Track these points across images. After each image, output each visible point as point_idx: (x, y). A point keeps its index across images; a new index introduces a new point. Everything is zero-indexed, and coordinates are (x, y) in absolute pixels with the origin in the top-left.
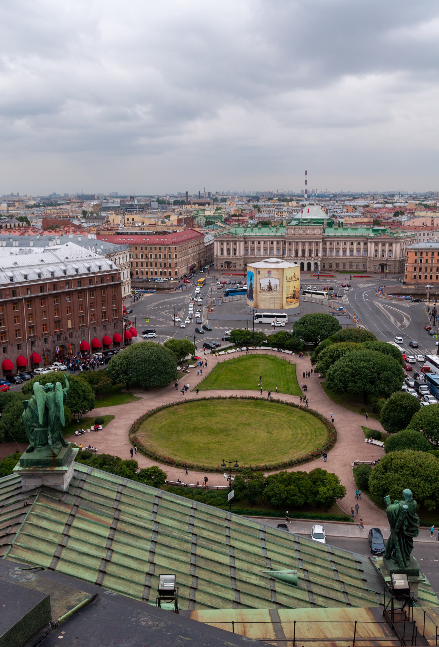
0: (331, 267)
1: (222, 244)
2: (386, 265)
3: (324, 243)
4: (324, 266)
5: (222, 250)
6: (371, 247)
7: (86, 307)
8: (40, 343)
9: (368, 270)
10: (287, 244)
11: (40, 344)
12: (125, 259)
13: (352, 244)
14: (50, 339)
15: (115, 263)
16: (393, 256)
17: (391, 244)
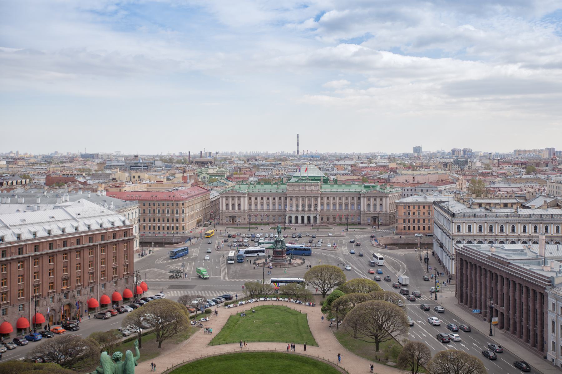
0: (328, 220)
1: (227, 199)
2: (378, 217)
3: (322, 198)
4: (322, 220)
5: (227, 205)
6: (364, 202)
7: (97, 263)
9: (362, 222)
10: (288, 199)
11: (45, 303)
12: (134, 214)
13: (347, 199)
14: (57, 297)
15: (128, 219)
16: (384, 209)
17: (381, 199)
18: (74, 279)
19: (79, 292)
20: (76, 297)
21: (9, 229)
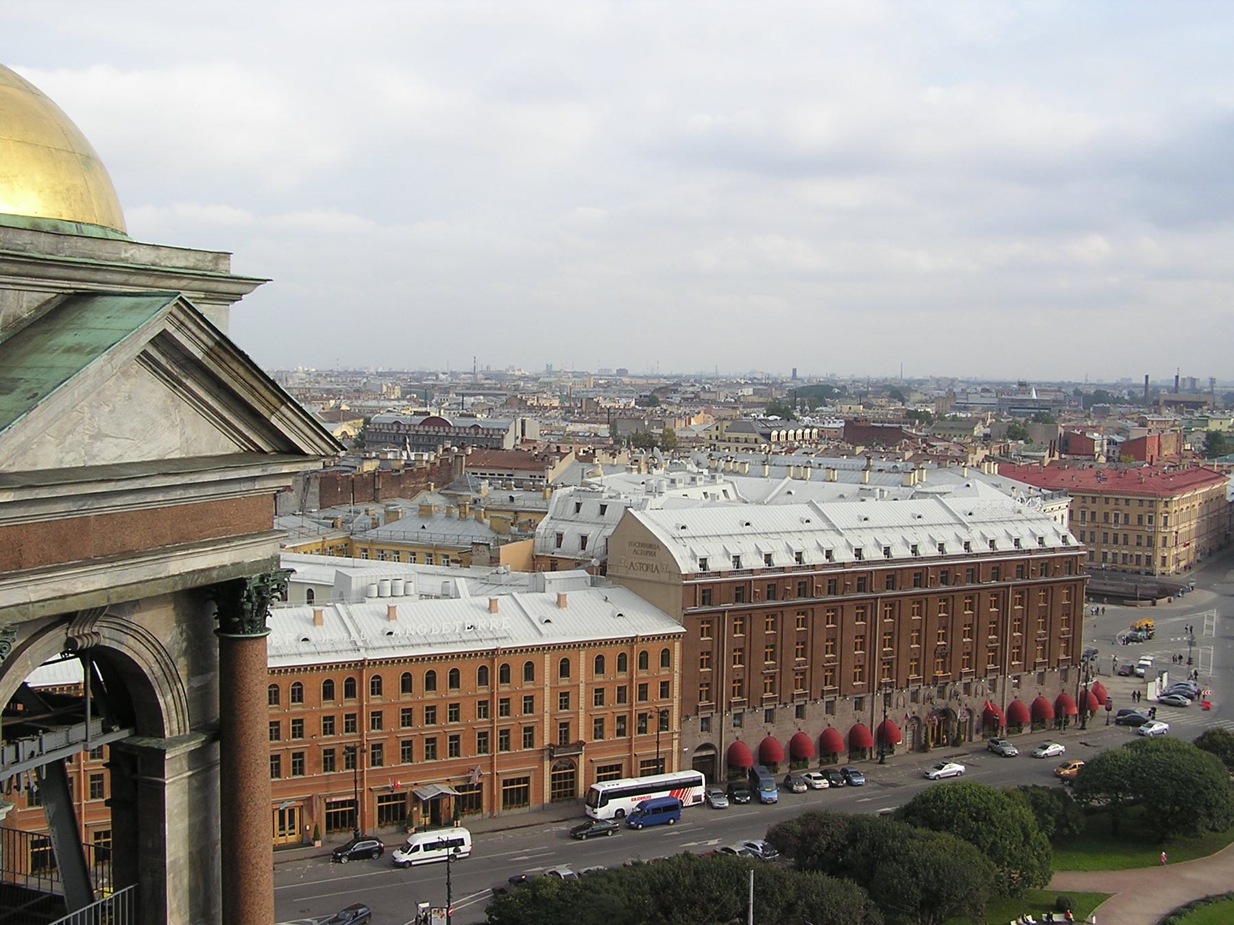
8: (902, 697)
18: (958, 656)
19: (967, 687)
20: (962, 696)
21: (841, 534)
